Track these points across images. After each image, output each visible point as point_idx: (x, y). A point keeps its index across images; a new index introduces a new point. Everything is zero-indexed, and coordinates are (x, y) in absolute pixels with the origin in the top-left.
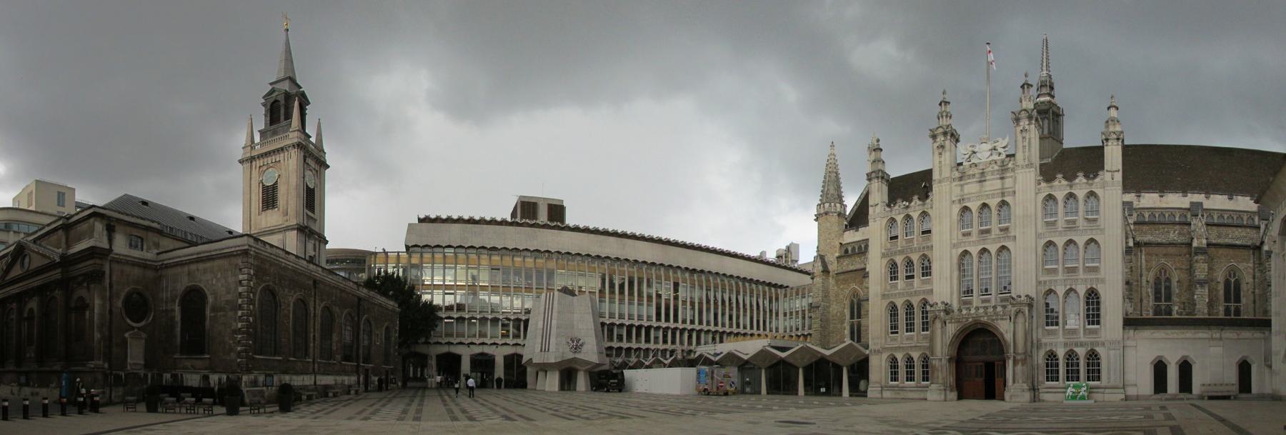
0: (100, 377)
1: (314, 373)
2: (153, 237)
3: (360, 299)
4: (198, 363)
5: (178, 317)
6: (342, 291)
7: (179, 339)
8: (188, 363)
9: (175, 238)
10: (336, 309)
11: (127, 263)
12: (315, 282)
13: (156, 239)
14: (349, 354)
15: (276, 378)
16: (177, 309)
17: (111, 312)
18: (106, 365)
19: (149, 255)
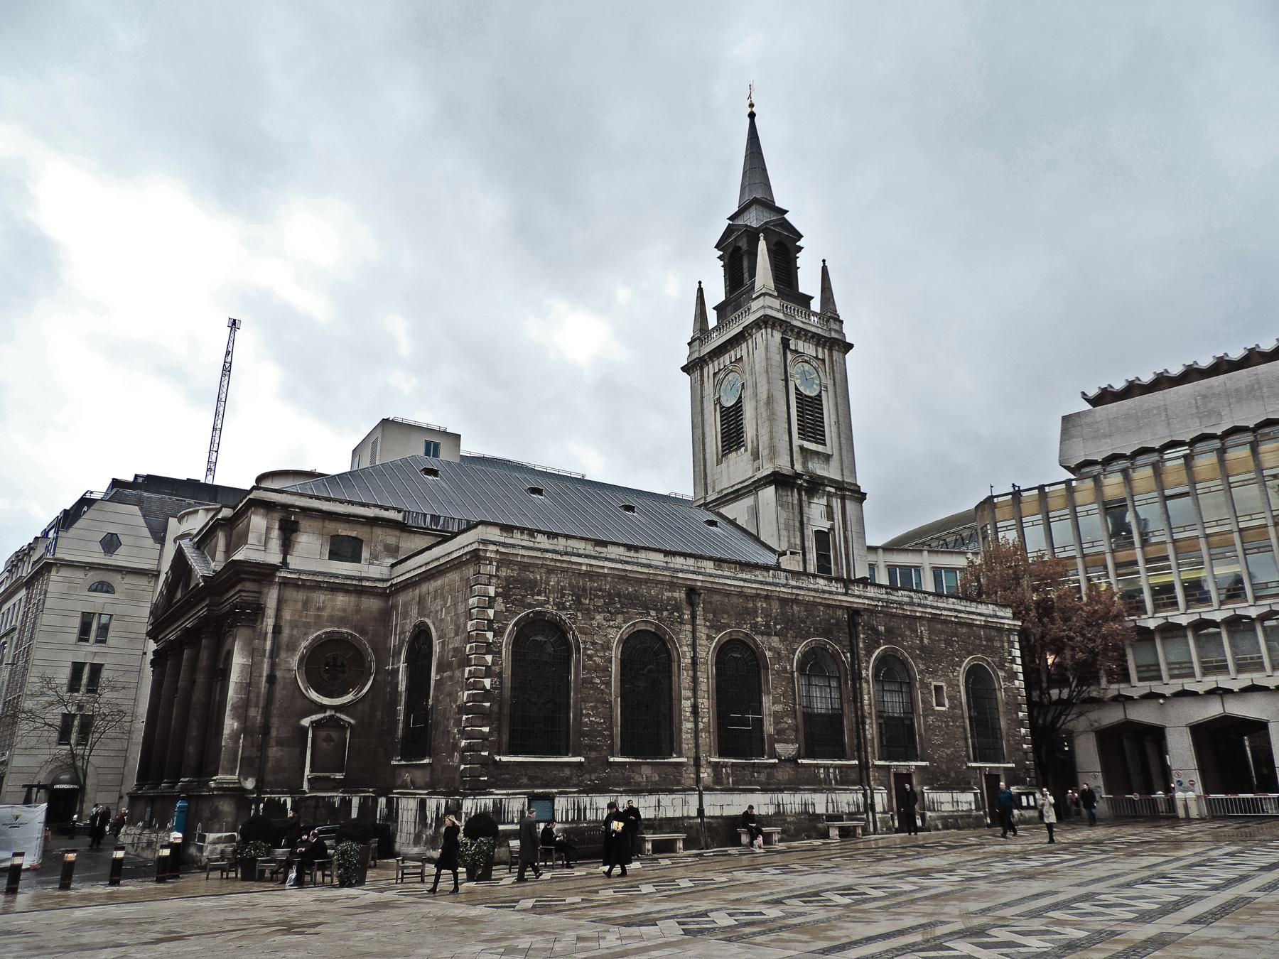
0: (226, 807)
1: (700, 788)
2: (382, 535)
3: (854, 613)
4: (420, 776)
5: (402, 687)
6: (784, 601)
7: (401, 726)
8: (407, 777)
9: (424, 532)
10: (770, 645)
11: (317, 586)
12: (692, 591)
13: (392, 540)
14: (823, 735)
15: (561, 804)
16: (402, 666)
17: (271, 679)
18: (250, 784)
19: (372, 569)
